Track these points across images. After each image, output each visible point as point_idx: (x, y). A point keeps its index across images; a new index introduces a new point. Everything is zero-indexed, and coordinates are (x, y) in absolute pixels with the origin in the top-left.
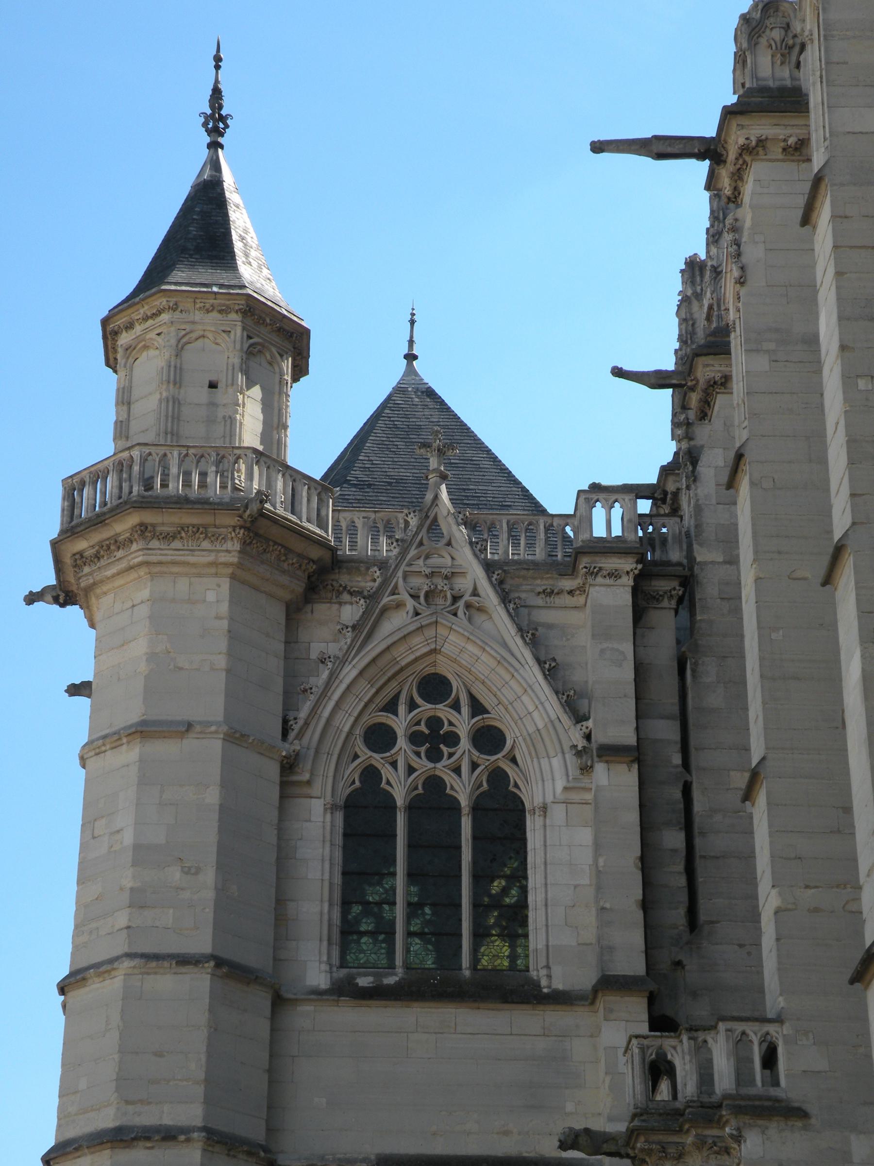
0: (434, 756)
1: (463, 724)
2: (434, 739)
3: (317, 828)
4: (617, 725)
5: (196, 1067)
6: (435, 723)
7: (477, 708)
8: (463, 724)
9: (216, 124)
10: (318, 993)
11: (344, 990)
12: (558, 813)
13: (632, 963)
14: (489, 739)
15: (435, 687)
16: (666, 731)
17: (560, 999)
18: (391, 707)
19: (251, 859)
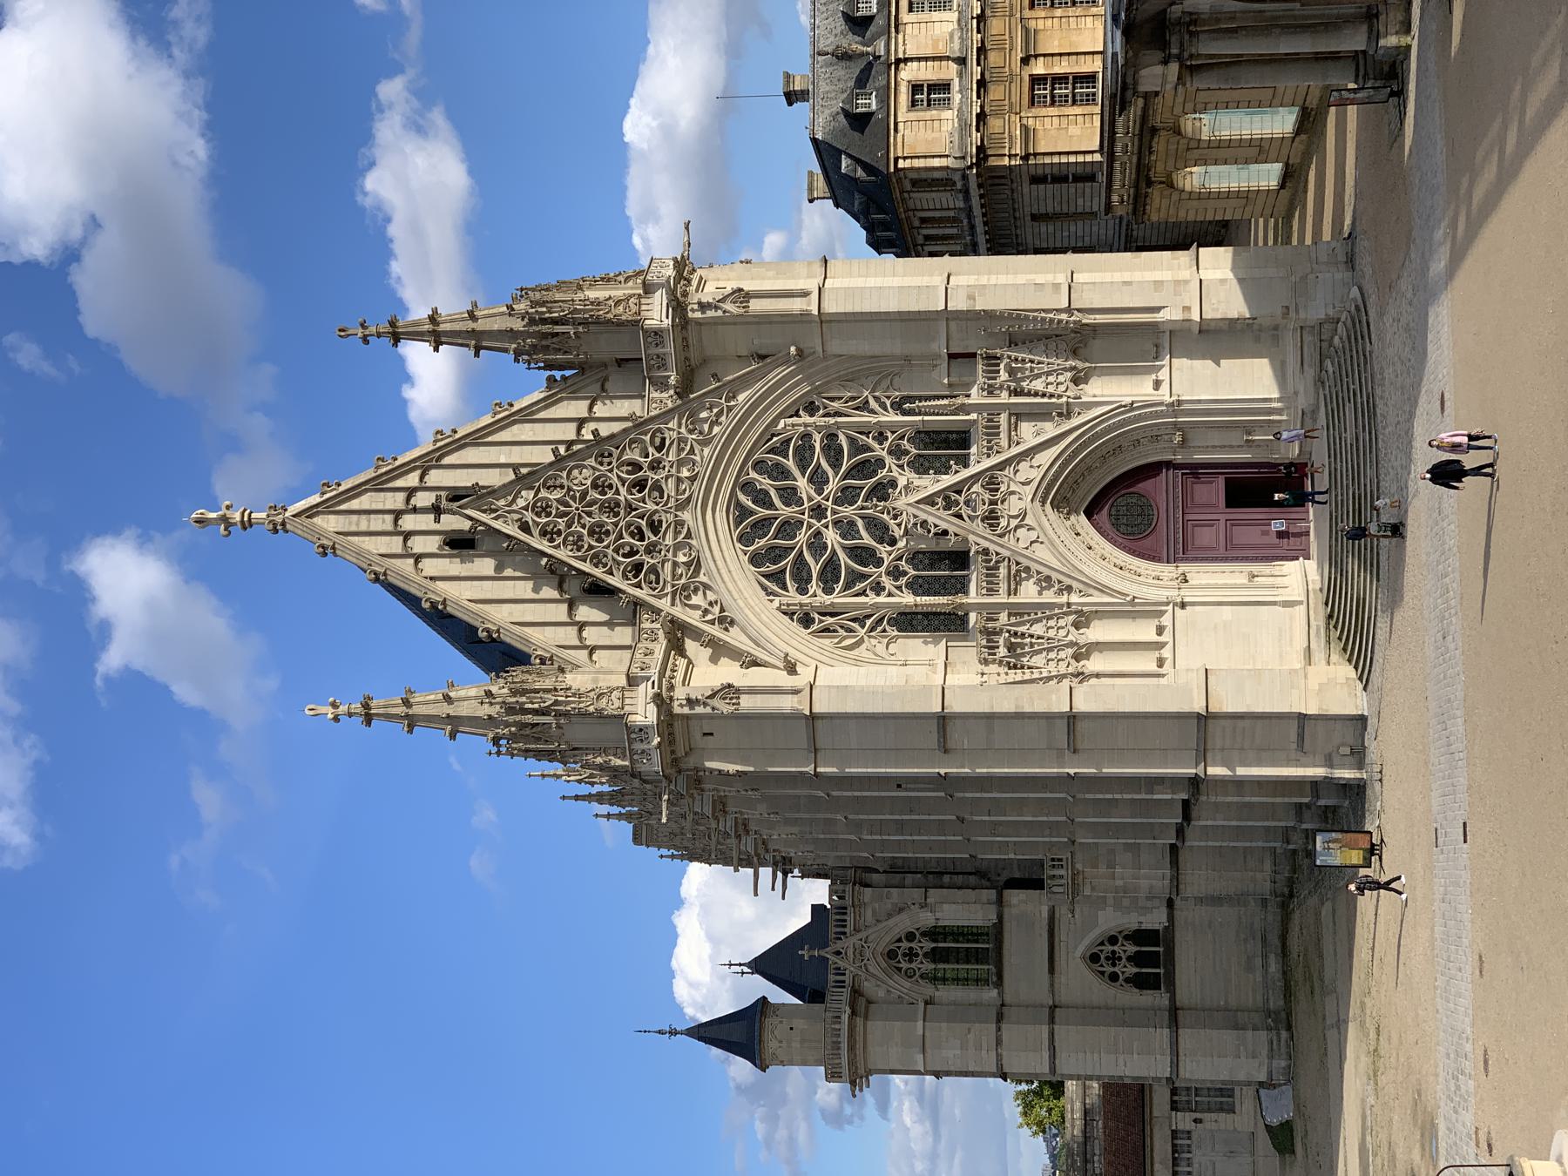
0: (917, 955)
1: (905, 945)
2: (911, 955)
3: (946, 993)
4: (917, 893)
5: (1030, 1028)
6: (905, 955)
7: (900, 940)
8: (905, 945)
9: (673, 1032)
10: (1001, 994)
11: (999, 983)
12: (938, 915)
13: (992, 894)
14: (910, 937)
15: (892, 955)
16: (909, 878)
17: (1000, 917)
18: (899, 969)
19: (961, 1014)
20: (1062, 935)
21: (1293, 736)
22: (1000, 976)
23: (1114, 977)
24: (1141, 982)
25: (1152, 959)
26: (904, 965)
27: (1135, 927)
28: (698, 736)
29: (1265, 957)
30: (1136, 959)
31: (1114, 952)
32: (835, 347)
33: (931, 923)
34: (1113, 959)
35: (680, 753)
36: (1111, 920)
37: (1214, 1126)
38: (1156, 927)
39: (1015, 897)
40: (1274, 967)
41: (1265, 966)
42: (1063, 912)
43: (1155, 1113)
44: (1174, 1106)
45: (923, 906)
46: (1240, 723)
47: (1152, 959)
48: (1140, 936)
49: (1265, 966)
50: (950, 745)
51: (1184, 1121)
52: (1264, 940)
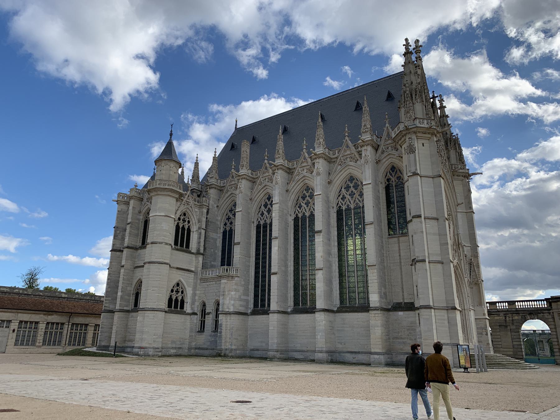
9: (171, 135)
13: (202, 251)
14: (189, 222)
15: (185, 214)
17: (193, 253)
20: (186, 274)
22: (177, 250)
23: (172, 291)
24: (170, 300)
25: (176, 307)
26: (182, 218)
27: (185, 301)
28: (423, 141)
29: (175, 348)
30: (177, 300)
31: (179, 292)
32: (459, 215)
33: (192, 230)
34: (177, 292)
35: (419, 135)
36: (189, 291)
37: (10, 337)
38: (185, 309)
39: (201, 258)
40: (173, 351)
41: (173, 348)
42: (192, 275)
43: (19, 314)
44: (21, 322)
45: (199, 228)
46: (446, 322)
47: (176, 307)
48: (183, 302)
49: (173, 348)
50: (427, 221)
51: (14, 325)
52: (180, 348)
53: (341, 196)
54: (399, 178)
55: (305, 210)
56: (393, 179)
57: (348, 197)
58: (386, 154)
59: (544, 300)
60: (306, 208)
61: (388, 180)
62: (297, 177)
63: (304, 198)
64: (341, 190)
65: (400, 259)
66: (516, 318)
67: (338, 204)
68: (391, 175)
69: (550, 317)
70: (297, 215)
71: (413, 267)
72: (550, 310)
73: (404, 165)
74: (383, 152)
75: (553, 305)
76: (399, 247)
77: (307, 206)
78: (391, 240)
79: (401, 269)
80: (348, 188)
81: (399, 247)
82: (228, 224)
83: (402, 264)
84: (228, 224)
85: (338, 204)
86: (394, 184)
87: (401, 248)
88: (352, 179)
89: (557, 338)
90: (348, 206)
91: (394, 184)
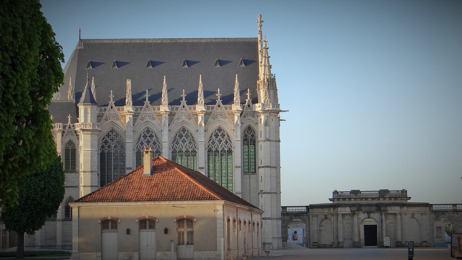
21: (274, 236)
35: (272, 114)
53: (211, 141)
54: (253, 136)
55: (182, 146)
56: (249, 136)
57: (217, 142)
58: (246, 118)
59: (304, 207)
60: (183, 145)
61: (246, 136)
62: (176, 121)
63: (181, 136)
64: (211, 136)
65: (250, 189)
66: (286, 218)
67: (209, 146)
68: (247, 131)
69: (307, 218)
70: (174, 149)
71: (260, 195)
72: (307, 213)
73: (259, 130)
74: (244, 117)
75: (310, 210)
76: (250, 180)
77: (184, 144)
78: (245, 176)
79: (250, 194)
80: (217, 136)
81: (250, 180)
82: (106, 147)
83: (251, 192)
84: (106, 147)
85: (209, 146)
86: (249, 139)
87: (251, 182)
88: (220, 129)
89: (309, 231)
90: (217, 149)
91: (249, 139)
